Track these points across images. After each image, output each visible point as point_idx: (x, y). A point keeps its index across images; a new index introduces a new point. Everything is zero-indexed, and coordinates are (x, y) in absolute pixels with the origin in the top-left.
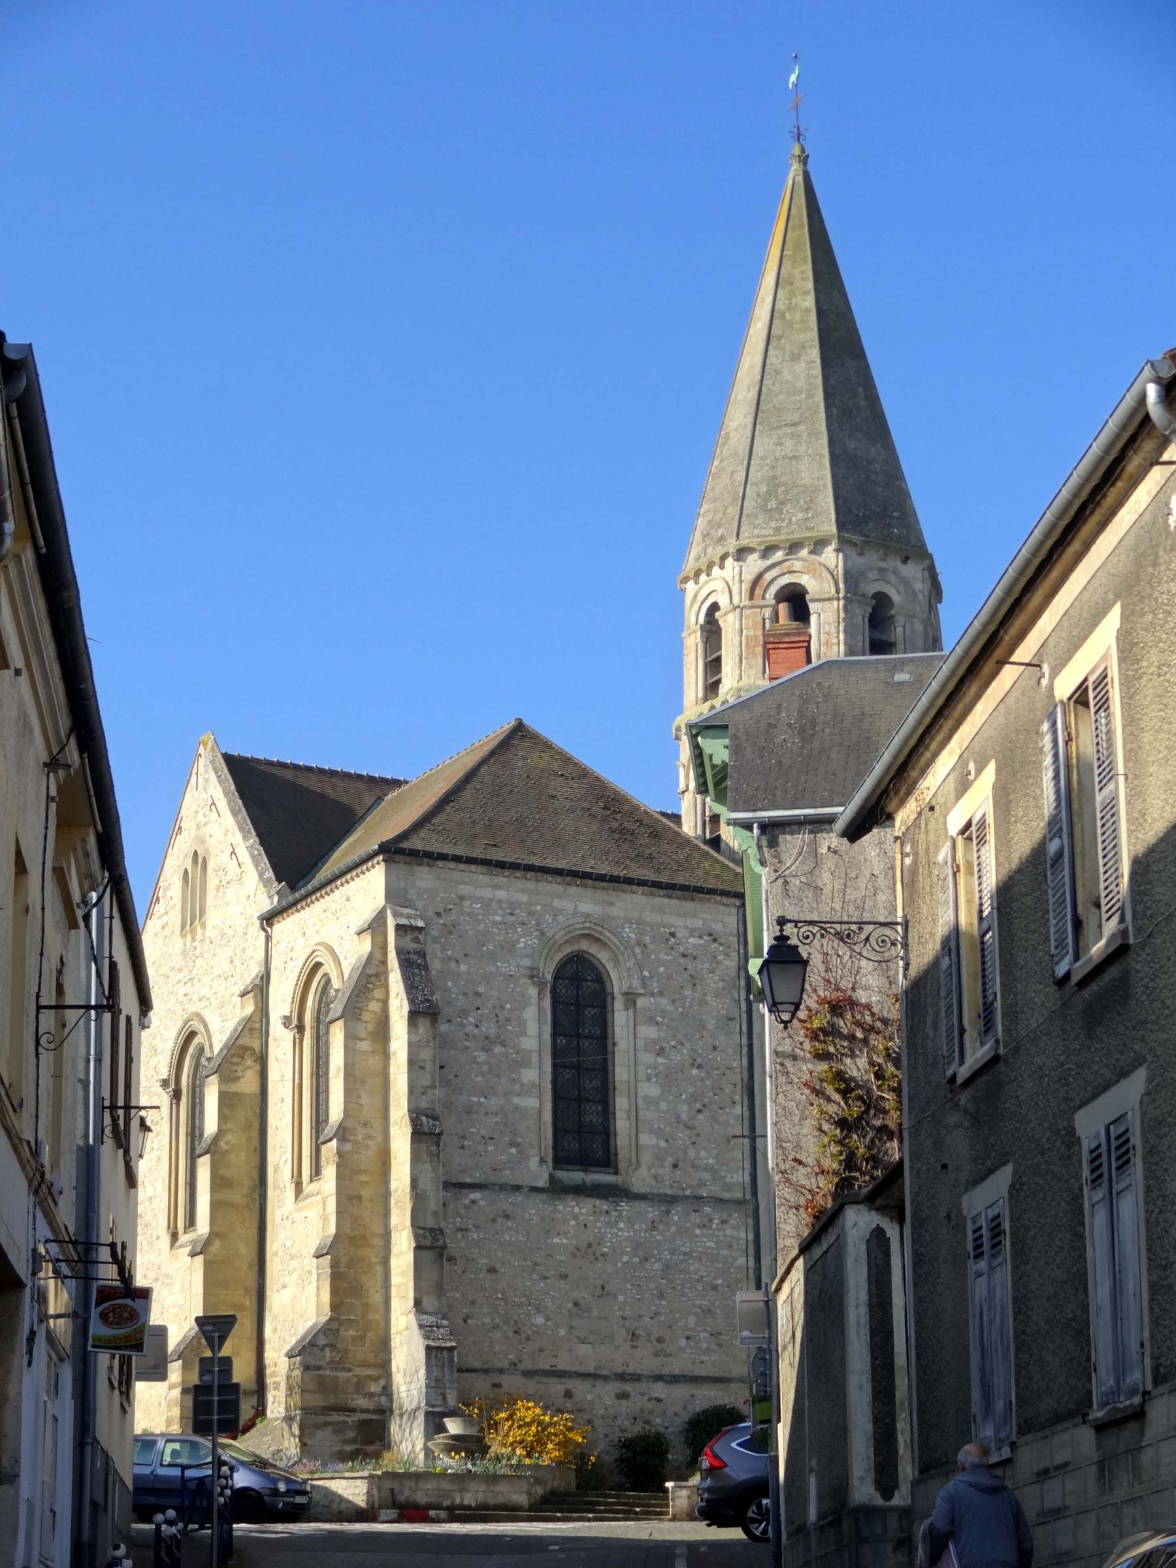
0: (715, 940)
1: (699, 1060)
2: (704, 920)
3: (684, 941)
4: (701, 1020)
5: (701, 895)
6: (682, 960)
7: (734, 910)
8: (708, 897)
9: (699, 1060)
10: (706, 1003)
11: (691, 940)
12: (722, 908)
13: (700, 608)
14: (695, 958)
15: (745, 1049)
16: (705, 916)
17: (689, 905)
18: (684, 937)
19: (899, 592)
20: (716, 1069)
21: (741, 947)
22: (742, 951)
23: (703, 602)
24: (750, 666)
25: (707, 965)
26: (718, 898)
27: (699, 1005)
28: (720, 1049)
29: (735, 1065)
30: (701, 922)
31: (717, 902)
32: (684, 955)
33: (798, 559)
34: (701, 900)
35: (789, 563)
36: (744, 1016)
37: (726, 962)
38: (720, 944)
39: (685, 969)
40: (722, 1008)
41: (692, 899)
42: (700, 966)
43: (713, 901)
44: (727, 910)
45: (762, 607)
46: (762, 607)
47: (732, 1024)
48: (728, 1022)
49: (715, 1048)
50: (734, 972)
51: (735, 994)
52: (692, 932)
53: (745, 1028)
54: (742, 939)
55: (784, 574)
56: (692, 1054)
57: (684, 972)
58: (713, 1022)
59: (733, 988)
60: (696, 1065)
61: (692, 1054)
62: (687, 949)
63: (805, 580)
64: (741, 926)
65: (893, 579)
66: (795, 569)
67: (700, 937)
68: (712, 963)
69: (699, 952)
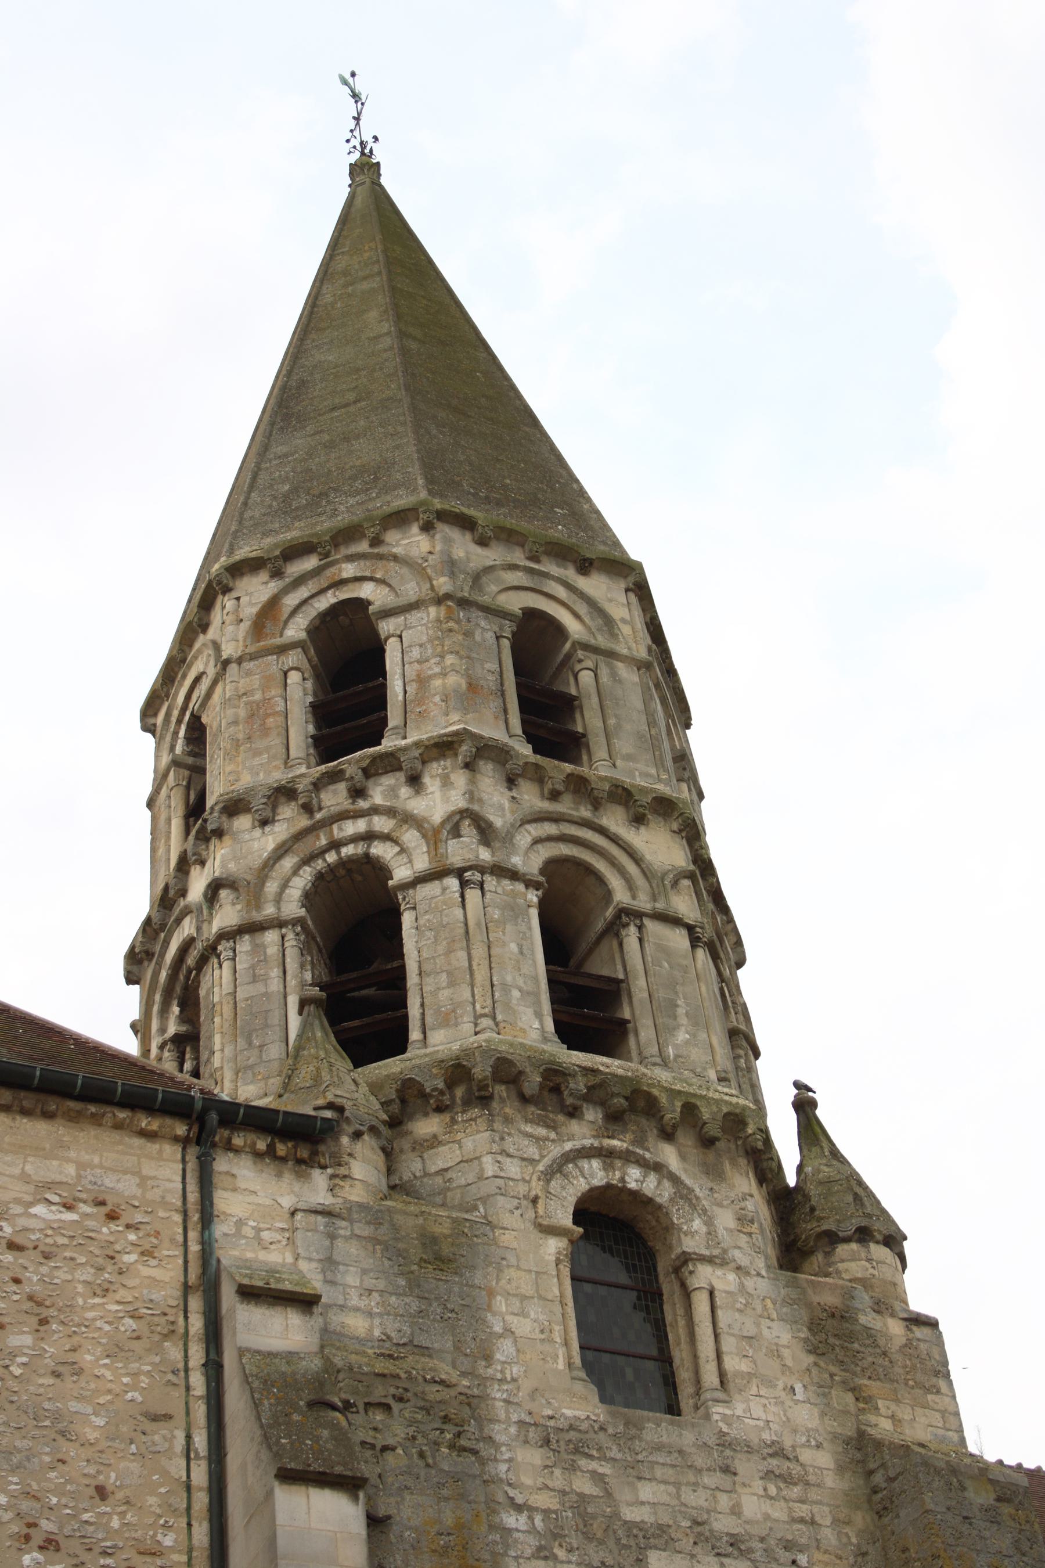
0: (112, 1217)
1: (46, 1525)
2: (81, 1166)
3: (17, 1209)
4: (57, 1416)
5: (72, 1104)
6: (9, 1257)
7: (171, 1151)
8: (92, 1109)
9: (46, 1525)
10: (79, 1372)
11: (39, 1210)
12: (137, 1142)
13: (176, 733)
14: (47, 1256)
15: (201, 1500)
16: (86, 1157)
17: (37, 1129)
18: (18, 1201)
19: (577, 616)
20: (105, 1553)
21: (193, 1235)
22: (194, 1247)
23: (179, 721)
24: (257, 753)
25: (86, 1274)
26: (122, 1115)
27: (57, 1375)
28: (120, 1495)
29: (168, 1541)
30: (71, 1170)
31: (118, 1126)
32: (13, 1246)
33: (350, 558)
34: (74, 1118)
35: (333, 570)
36: (200, 1411)
37: (145, 1271)
38: (128, 1226)
39: (17, 1281)
40: (134, 1387)
41: (48, 1116)
42: (62, 1275)
43: (108, 1119)
44: (153, 1147)
45: (282, 650)
46: (282, 650)
47: (159, 1434)
48: (148, 1426)
49: (102, 1492)
50: (168, 1294)
51: (174, 1352)
52: (42, 1190)
53: (200, 1441)
54: (195, 1217)
55: (322, 591)
56: (25, 1505)
57: (14, 1287)
58: (100, 1422)
59: (166, 1336)
60: (38, 1539)
61: (25, 1505)
62: (26, 1230)
63: (366, 591)
64: (193, 1188)
65: (561, 592)
66: (345, 575)
67: (69, 1207)
68: (100, 1269)
69: (61, 1240)
